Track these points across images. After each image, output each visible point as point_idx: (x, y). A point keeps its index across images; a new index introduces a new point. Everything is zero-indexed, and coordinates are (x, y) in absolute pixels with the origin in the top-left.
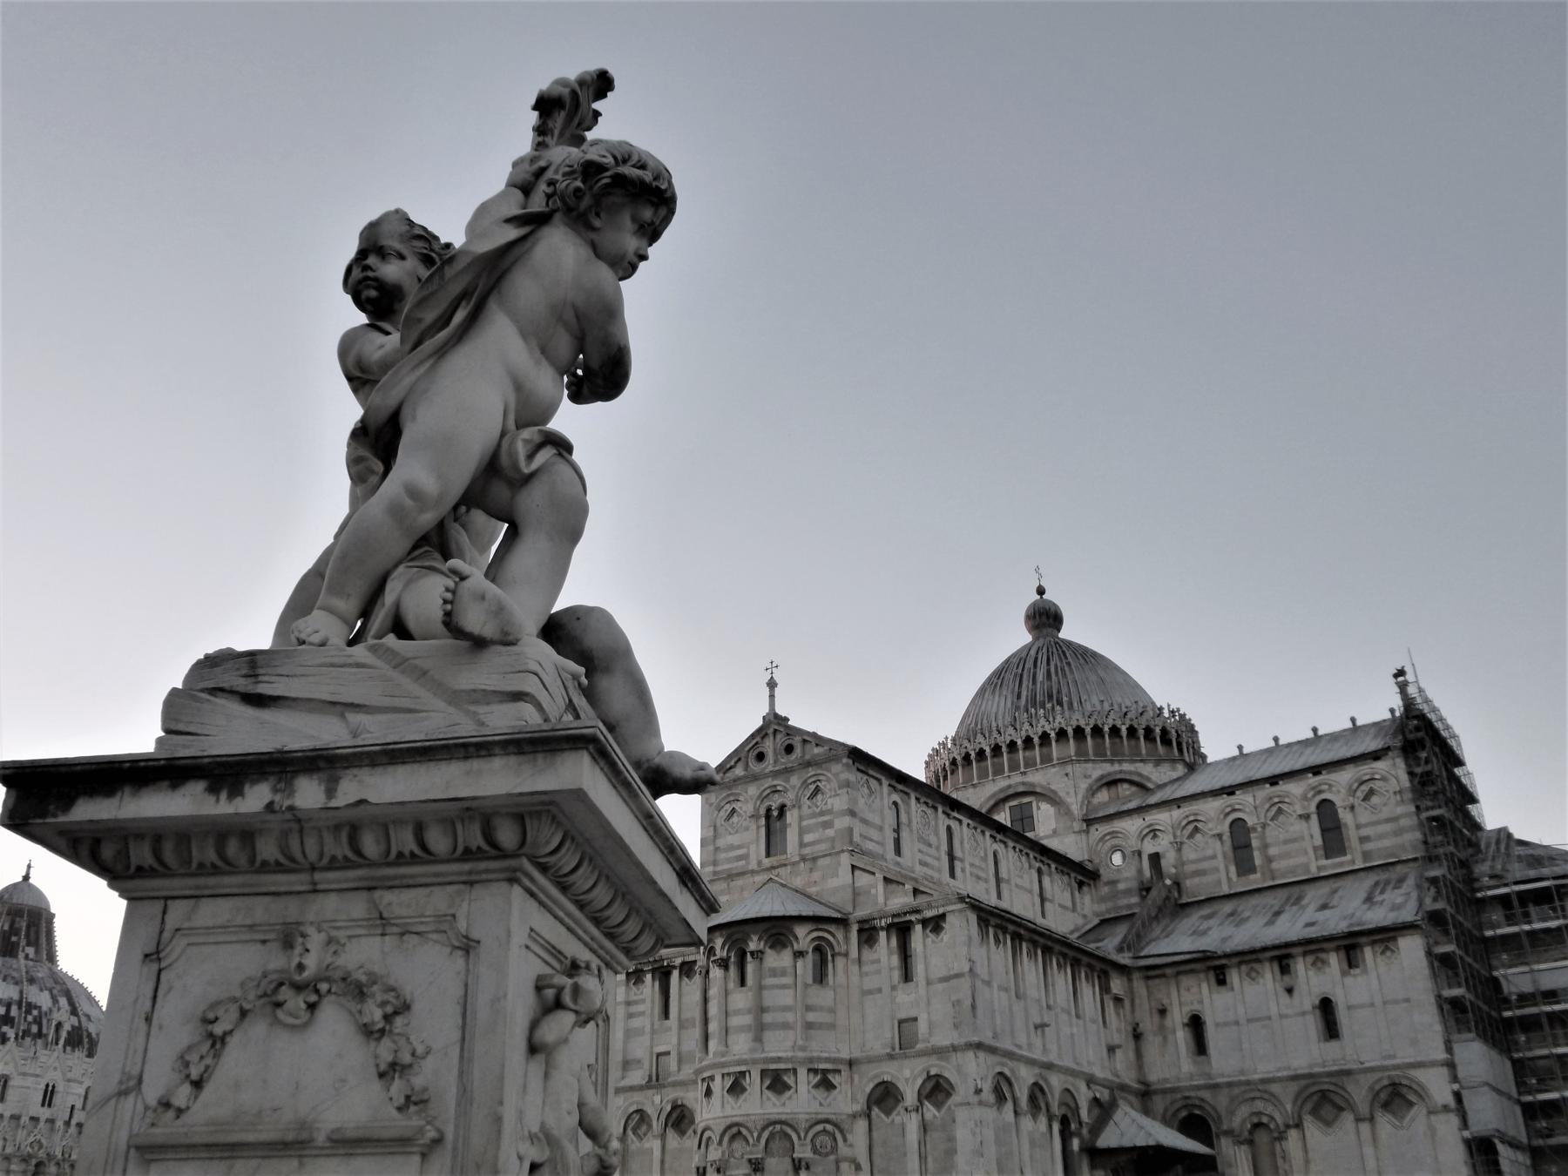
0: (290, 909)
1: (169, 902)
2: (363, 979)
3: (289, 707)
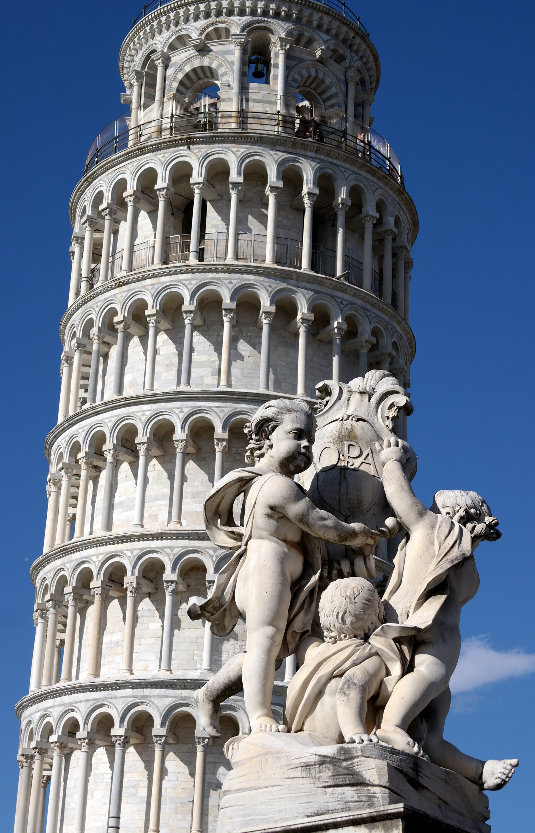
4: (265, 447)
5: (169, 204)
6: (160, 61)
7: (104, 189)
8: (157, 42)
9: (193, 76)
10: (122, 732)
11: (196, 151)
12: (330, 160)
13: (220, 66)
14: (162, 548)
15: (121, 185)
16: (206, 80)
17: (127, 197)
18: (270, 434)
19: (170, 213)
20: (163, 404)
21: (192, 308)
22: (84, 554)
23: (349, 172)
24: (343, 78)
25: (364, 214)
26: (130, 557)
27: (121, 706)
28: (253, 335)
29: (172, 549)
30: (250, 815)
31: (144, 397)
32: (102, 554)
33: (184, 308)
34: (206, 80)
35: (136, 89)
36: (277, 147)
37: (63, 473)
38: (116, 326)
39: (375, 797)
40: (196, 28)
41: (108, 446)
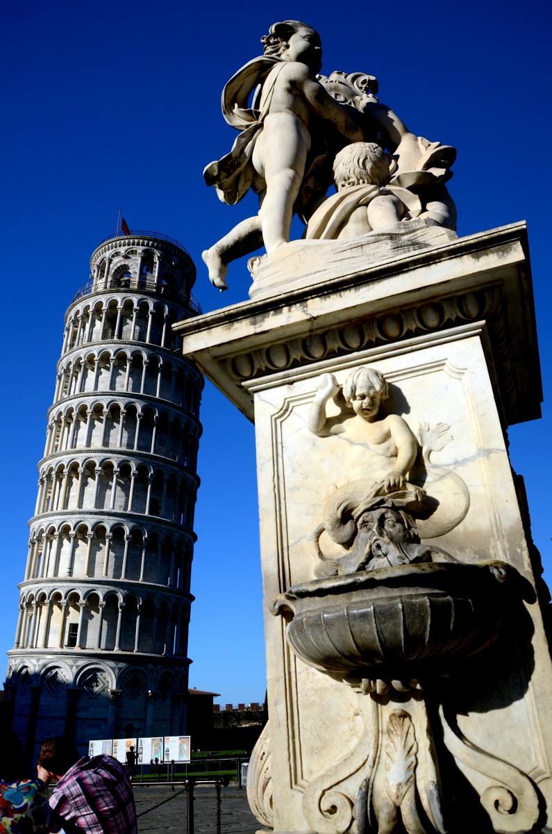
4: (282, 48)
7: (80, 309)
9: (121, 269)
10: (74, 532)
13: (132, 265)
14: (95, 456)
15: (88, 307)
21: (114, 358)
27: (74, 522)
35: (96, 272)
37: (54, 424)
41: (74, 414)
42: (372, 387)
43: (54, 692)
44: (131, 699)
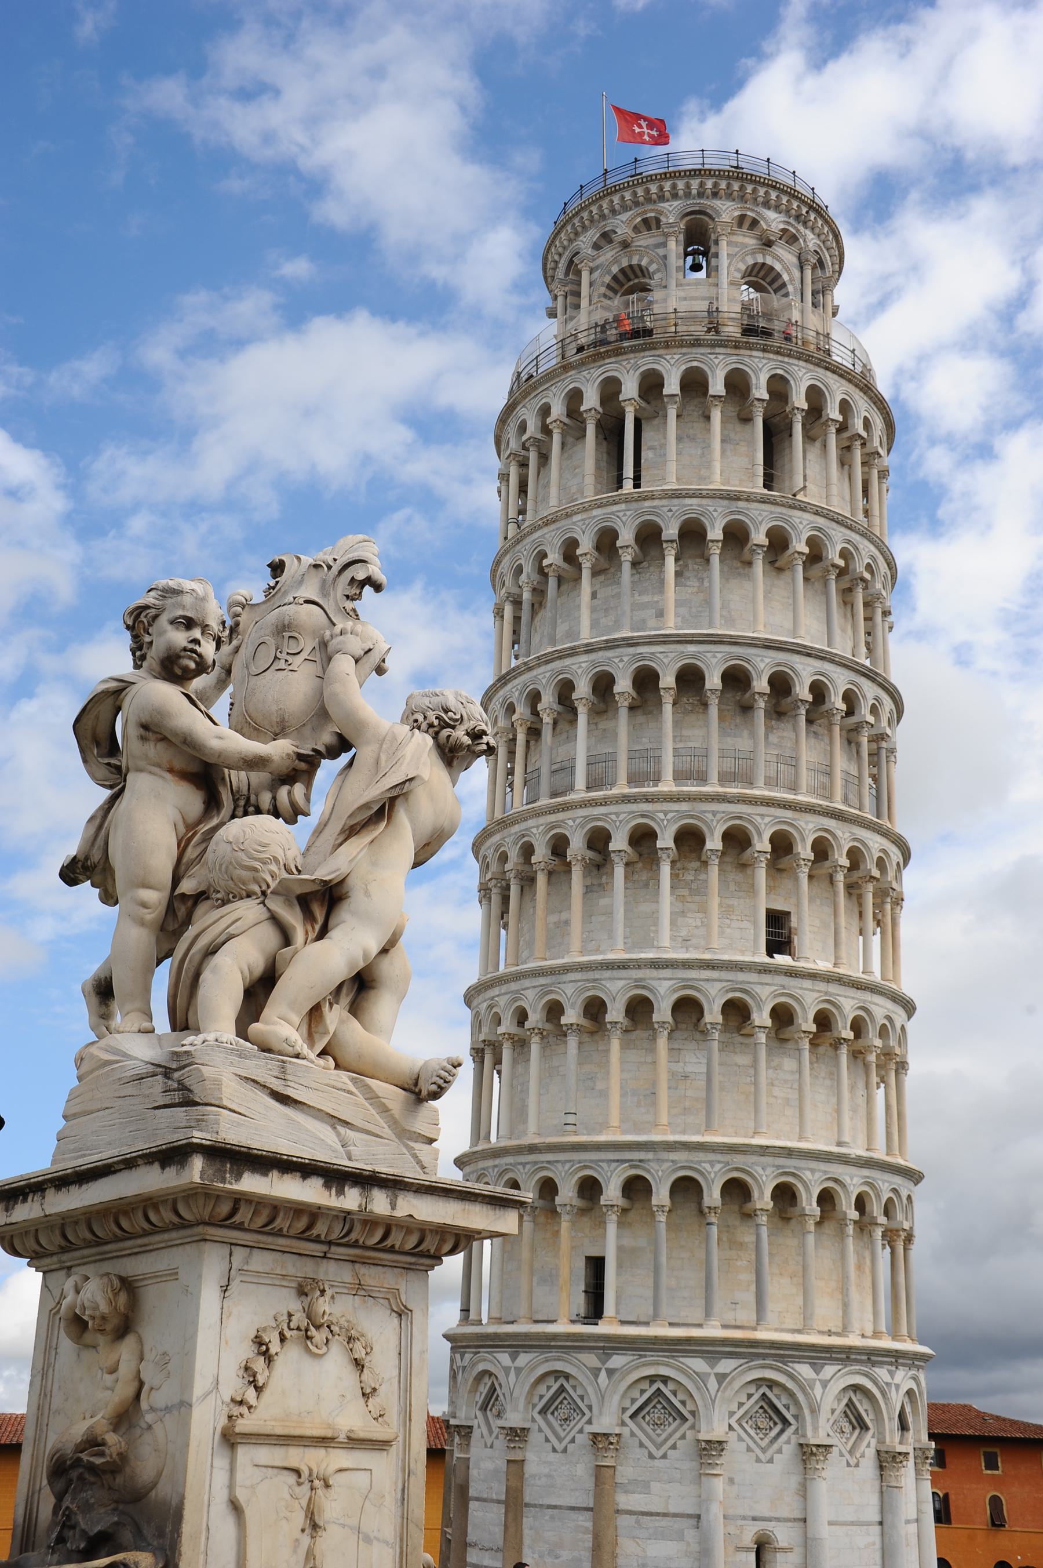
0: (306, 1269)
1: (233, 1247)
2: (346, 1325)
3: (302, 1111)
5: (600, 426)
6: (583, 264)
8: (580, 243)
9: (621, 277)
11: (624, 363)
12: (780, 358)
13: (651, 262)
14: (606, 815)
15: (545, 411)
16: (636, 281)
17: (551, 423)
18: (150, 625)
19: (601, 436)
20: (601, 654)
22: (523, 826)
23: (804, 371)
24: (795, 260)
25: (824, 419)
26: (572, 826)
27: (569, 989)
28: (701, 568)
29: (617, 814)
30: (81, 1150)
31: (579, 647)
32: (542, 825)
33: (619, 544)
34: (636, 281)
35: (560, 299)
36: (718, 350)
38: (546, 571)
39: (203, 1120)
40: (622, 222)
42: (96, 1308)
43: (560, 1440)
44: (758, 1460)
